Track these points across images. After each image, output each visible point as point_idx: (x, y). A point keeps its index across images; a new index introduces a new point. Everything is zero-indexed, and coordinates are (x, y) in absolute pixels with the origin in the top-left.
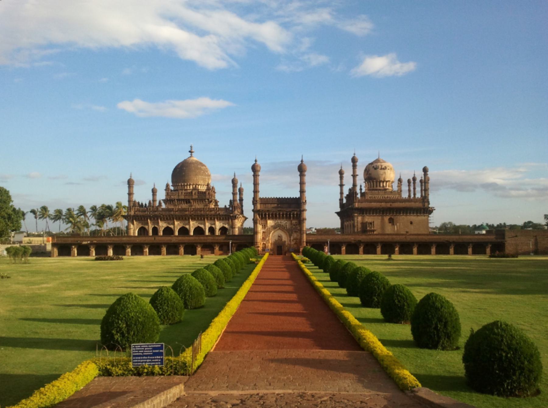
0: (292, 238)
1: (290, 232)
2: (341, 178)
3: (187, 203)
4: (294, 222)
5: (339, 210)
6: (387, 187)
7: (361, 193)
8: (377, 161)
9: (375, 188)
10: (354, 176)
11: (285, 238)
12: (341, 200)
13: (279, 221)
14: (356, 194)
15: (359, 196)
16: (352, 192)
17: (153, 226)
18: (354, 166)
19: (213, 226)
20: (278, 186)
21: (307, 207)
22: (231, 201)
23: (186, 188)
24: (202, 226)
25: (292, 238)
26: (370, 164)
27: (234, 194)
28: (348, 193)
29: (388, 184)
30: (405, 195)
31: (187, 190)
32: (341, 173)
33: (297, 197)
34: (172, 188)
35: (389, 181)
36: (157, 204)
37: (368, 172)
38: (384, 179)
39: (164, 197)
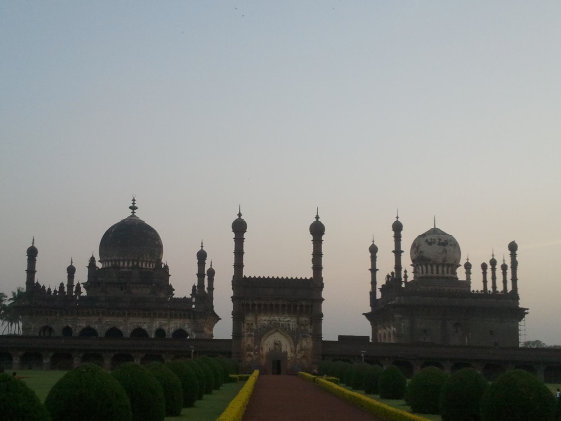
0: (298, 348)
1: (295, 336)
2: (374, 259)
3: (122, 289)
4: (303, 319)
5: (369, 310)
6: (450, 275)
7: (406, 282)
8: (435, 231)
9: (430, 274)
10: (398, 252)
11: (286, 346)
12: (373, 294)
13: (276, 318)
14: (401, 282)
15: (403, 285)
16: (394, 280)
17: (65, 325)
18: (398, 238)
19: (164, 328)
20: (278, 257)
21: (324, 294)
22: (194, 287)
23: (121, 264)
24: (145, 327)
25: (298, 348)
26: (420, 236)
27: (201, 275)
28: (384, 283)
29: (450, 269)
30: (476, 286)
31: (123, 267)
32: (373, 250)
33: (308, 278)
34: (99, 265)
35: (452, 265)
36: (74, 290)
37: (418, 248)
38: (445, 260)
39: (85, 280)
